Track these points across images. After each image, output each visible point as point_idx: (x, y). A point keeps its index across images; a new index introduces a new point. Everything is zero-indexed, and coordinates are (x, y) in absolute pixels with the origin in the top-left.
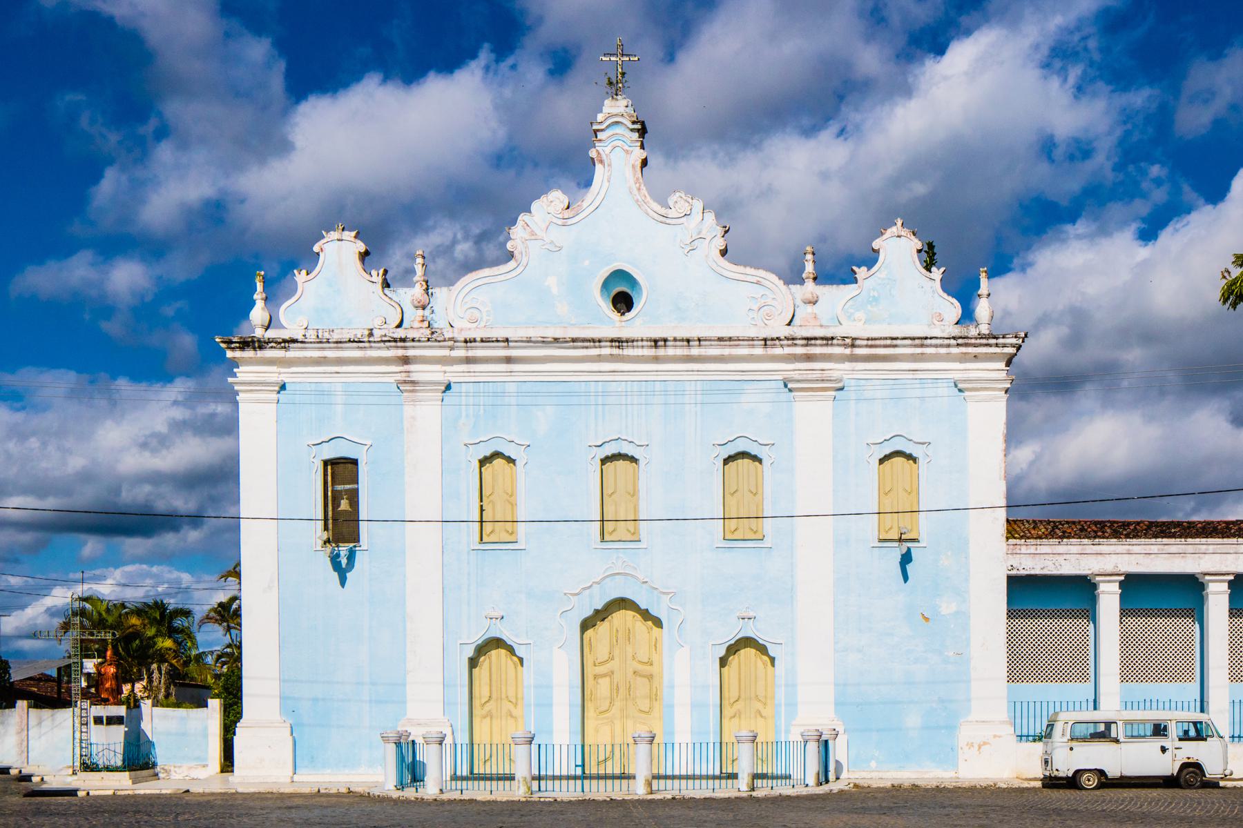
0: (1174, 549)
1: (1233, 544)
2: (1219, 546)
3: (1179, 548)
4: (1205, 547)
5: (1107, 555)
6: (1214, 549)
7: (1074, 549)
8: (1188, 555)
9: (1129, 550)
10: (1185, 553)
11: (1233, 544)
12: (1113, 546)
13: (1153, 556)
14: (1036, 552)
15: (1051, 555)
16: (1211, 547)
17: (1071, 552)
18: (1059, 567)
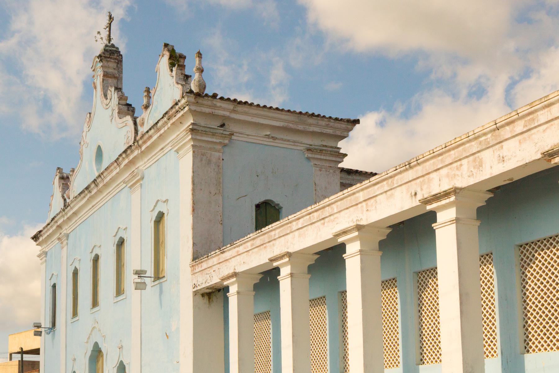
0: (258, 242)
1: (288, 224)
2: (281, 229)
3: (261, 240)
4: (273, 233)
5: (230, 260)
6: (279, 233)
7: (215, 260)
8: (268, 244)
9: (238, 252)
10: (265, 244)
11: (288, 224)
12: (231, 251)
13: (251, 252)
14: (201, 269)
15: (208, 269)
16: (277, 231)
17: (214, 264)
18: (212, 278)
